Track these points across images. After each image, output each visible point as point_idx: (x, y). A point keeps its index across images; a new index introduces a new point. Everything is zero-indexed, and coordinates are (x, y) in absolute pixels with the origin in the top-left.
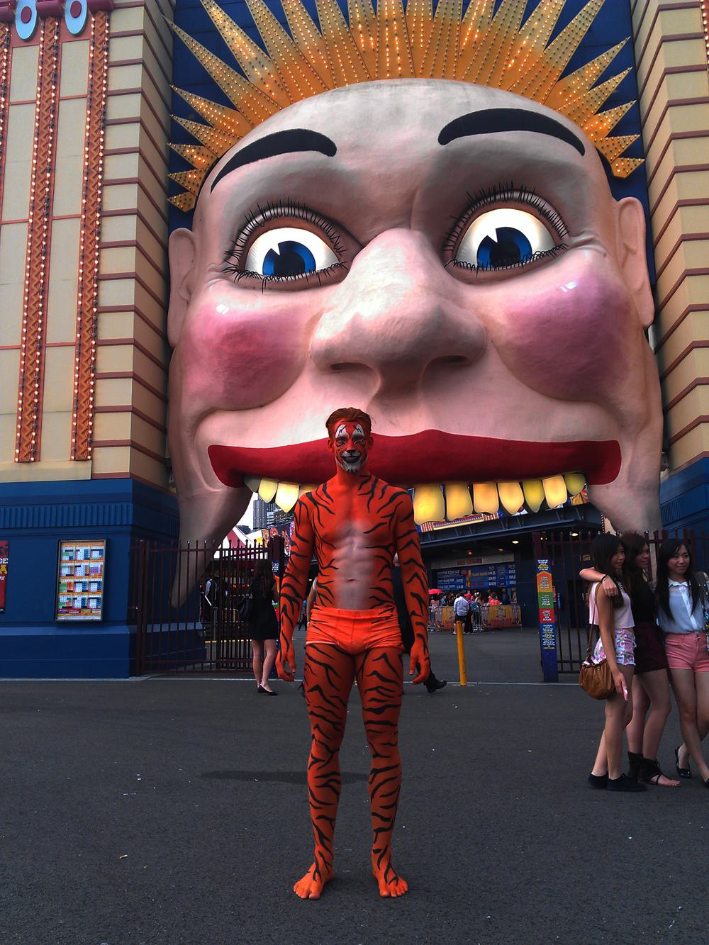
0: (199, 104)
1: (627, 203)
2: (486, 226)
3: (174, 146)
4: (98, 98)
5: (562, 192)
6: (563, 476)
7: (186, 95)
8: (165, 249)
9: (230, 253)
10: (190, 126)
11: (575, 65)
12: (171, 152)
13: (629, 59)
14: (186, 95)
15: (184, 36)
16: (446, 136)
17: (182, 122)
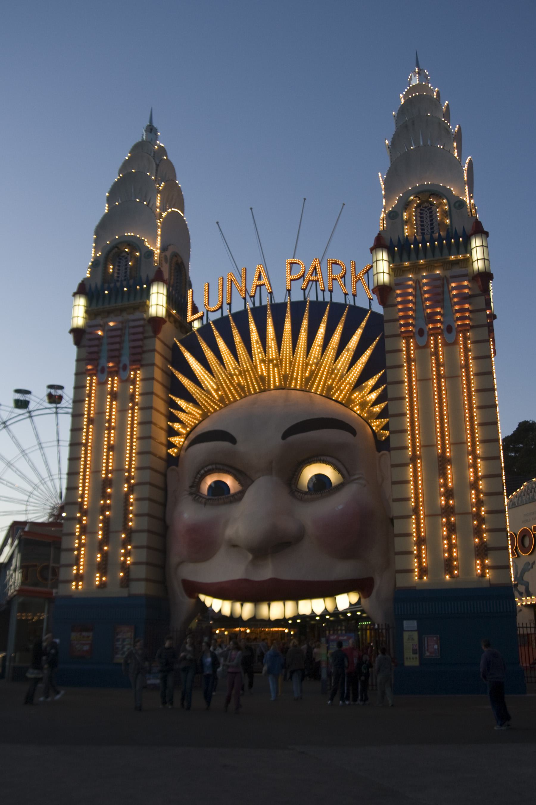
0: (181, 403)
1: (383, 454)
3: (171, 424)
6: (348, 595)
8: (165, 475)
9: (191, 487)
12: (169, 426)
16: (285, 436)
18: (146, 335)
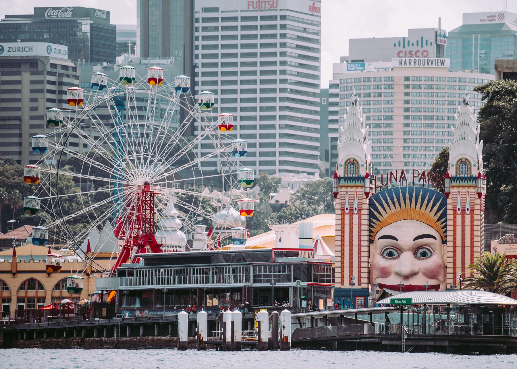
2: (421, 251)
4: (360, 225)
5: (432, 246)
7: (372, 219)
8: (369, 246)
10: (373, 225)
11: (438, 220)
13: (446, 221)
14: (372, 219)
15: (372, 210)
16: (414, 240)
17: (372, 224)
18: (363, 197)
